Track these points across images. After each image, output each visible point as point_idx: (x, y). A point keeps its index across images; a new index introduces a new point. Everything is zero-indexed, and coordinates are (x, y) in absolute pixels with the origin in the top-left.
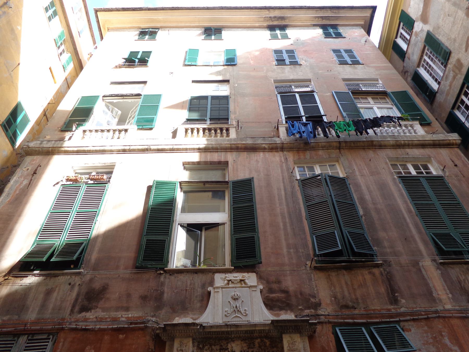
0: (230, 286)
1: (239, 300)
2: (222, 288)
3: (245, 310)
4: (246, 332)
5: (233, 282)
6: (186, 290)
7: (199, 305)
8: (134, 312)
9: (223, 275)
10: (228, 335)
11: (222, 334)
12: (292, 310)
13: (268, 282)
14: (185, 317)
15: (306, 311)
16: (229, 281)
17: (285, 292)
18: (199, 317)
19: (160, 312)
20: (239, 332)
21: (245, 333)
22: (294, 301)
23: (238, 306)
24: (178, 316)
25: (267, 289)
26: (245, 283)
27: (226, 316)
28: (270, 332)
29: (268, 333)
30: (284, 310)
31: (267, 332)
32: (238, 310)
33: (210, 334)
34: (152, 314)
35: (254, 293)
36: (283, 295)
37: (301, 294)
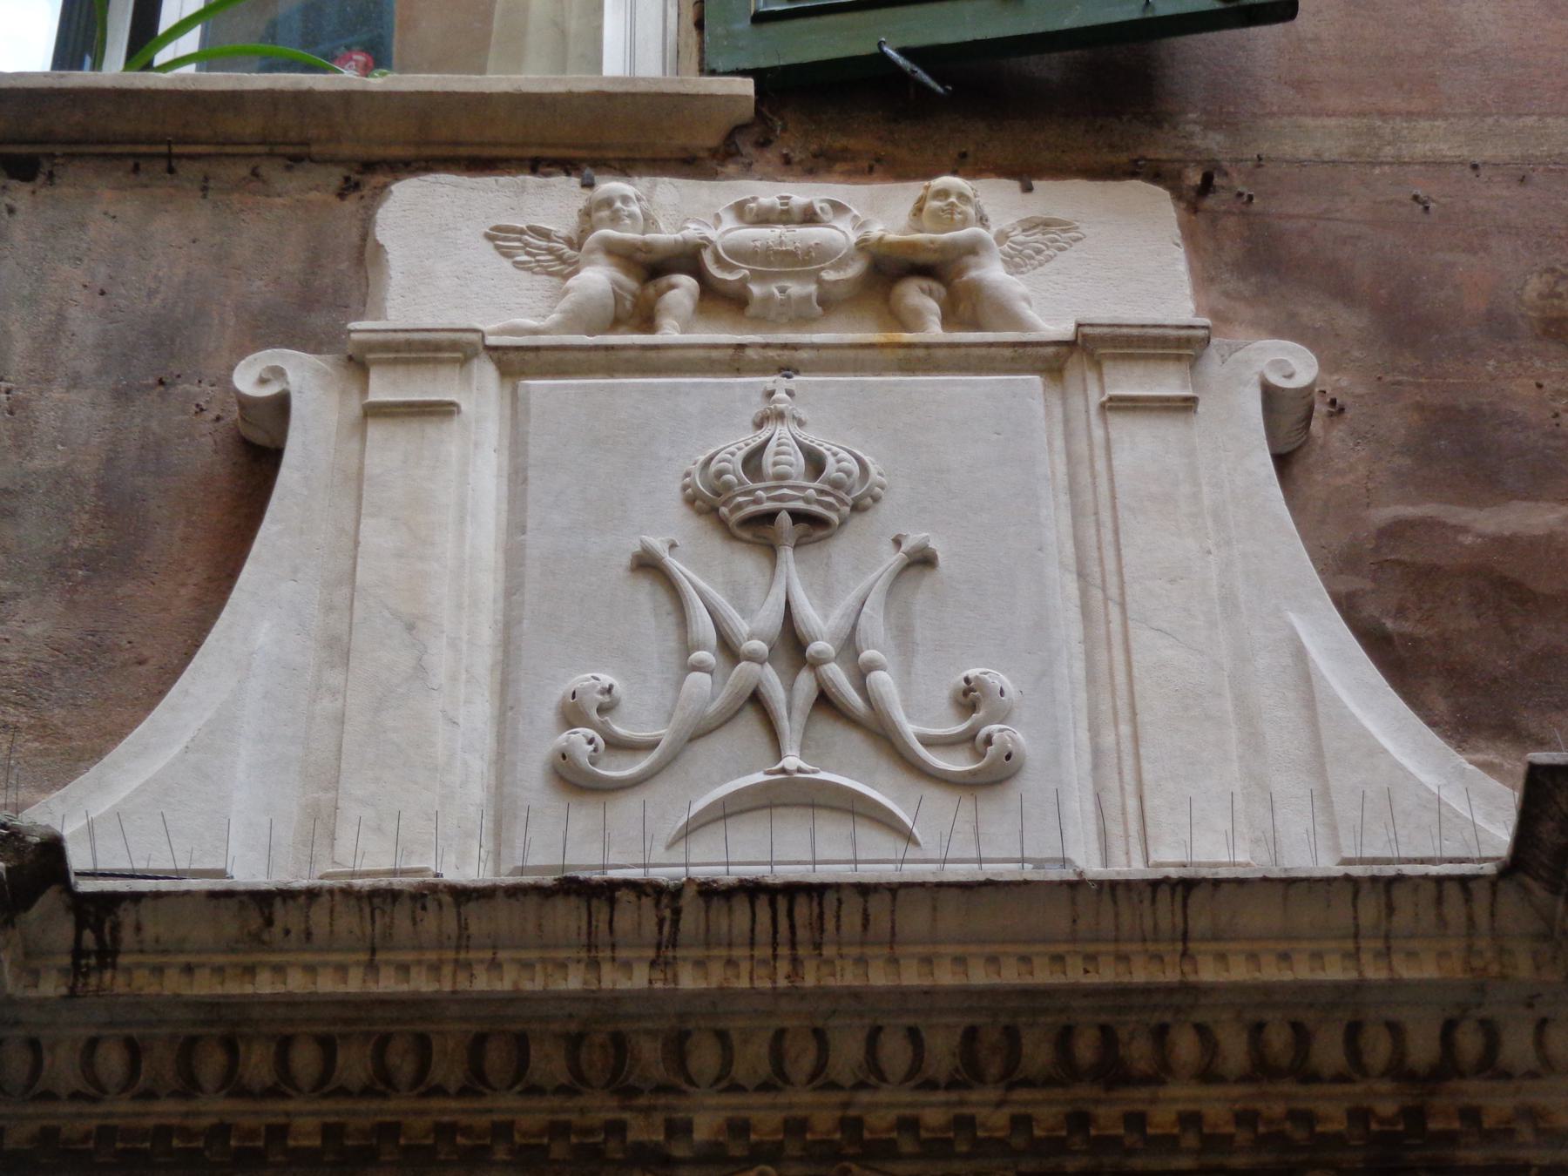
0: (670, 333)
1: (841, 549)
2: (516, 362)
3: (969, 698)
4: (991, 1038)
5: (720, 299)
10: (599, 1108)
11: (476, 1082)
13: (1405, 322)
20: (847, 1052)
21: (969, 1073)
23: (821, 625)
26: (966, 304)
27: (572, 780)
28: (1489, 1065)
29: (1447, 1067)
31: (1423, 1049)
32: (826, 701)
33: (232, 1084)
35: (1140, 447)
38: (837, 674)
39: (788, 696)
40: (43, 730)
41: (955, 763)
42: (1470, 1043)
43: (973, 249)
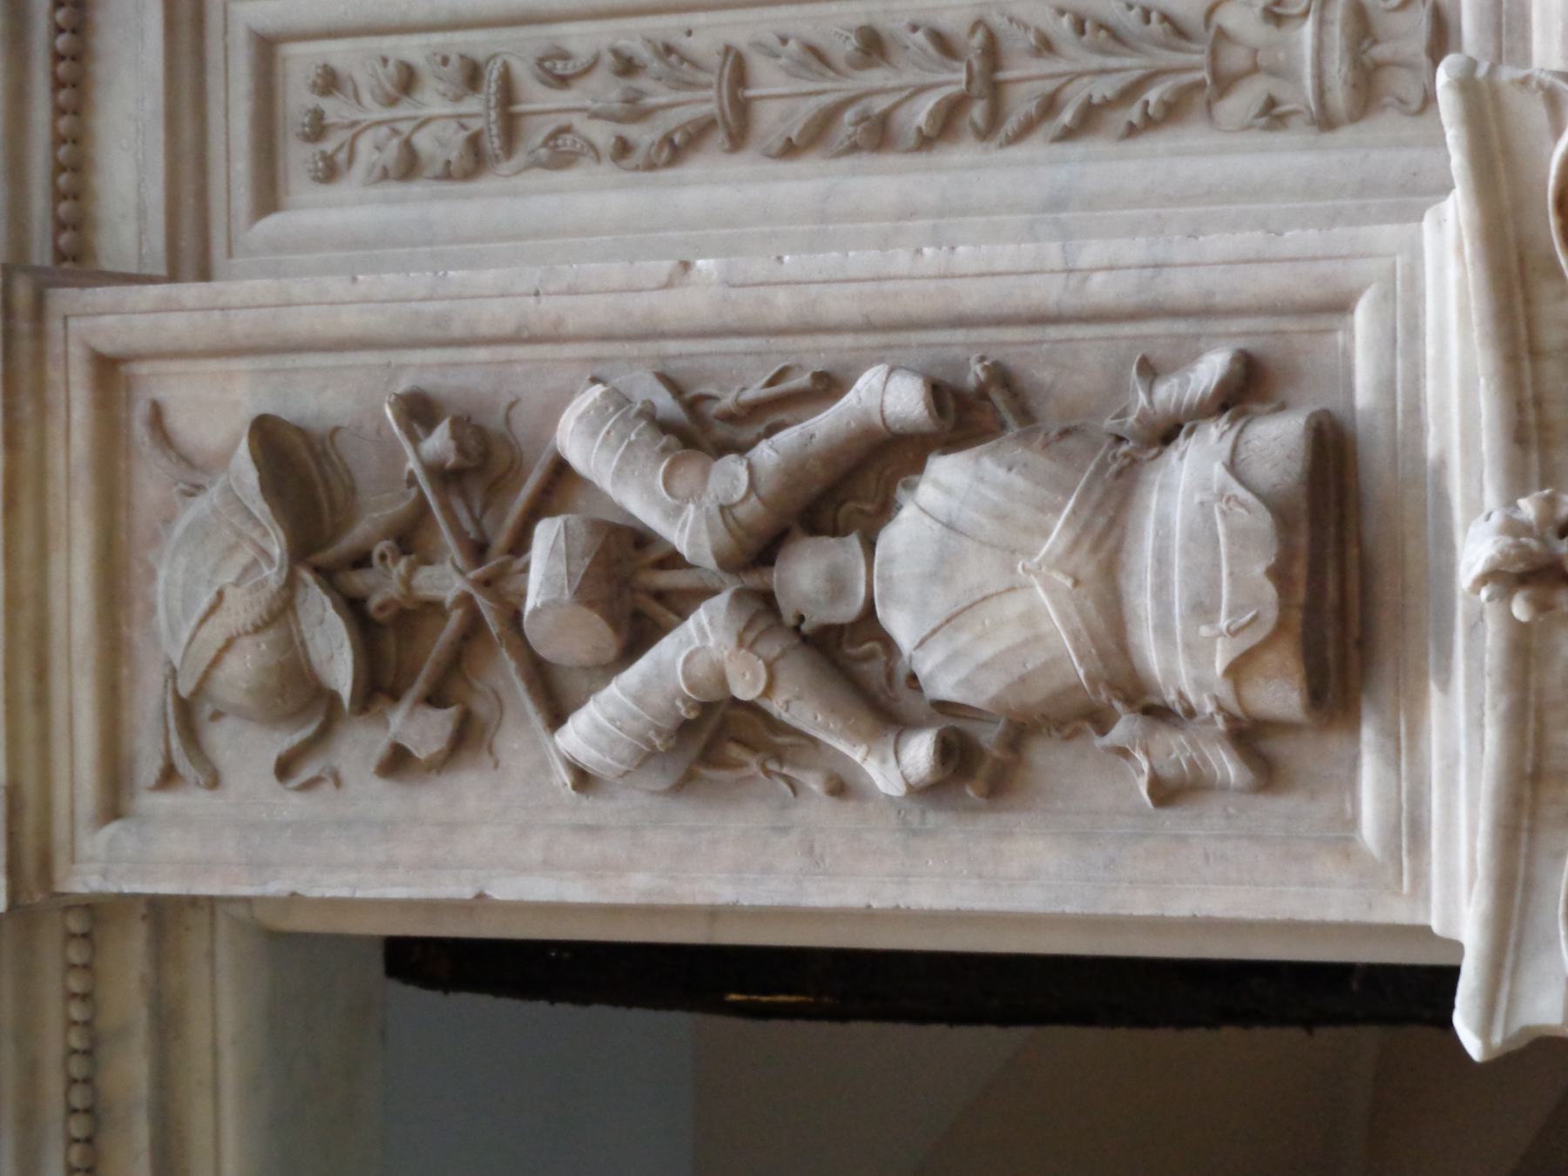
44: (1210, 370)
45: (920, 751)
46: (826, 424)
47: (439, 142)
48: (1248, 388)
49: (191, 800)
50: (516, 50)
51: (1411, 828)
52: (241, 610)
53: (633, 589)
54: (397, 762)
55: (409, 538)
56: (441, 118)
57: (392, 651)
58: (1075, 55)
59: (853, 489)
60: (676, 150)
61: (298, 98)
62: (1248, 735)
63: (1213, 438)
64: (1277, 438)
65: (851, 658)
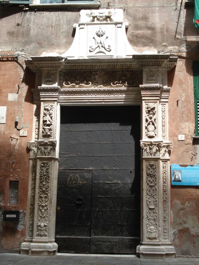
2: (87, 24)
5: (98, 19)
6: (52, 26)
7: (64, 40)
8: (4, 47)
9: (88, 11)
12: (155, 47)
13: (135, 19)
14: (51, 51)
15: (169, 48)
16: (94, 17)
17: (152, 29)
18: (64, 52)
19: (28, 47)
22: (158, 38)
24: (44, 51)
25: (133, 26)
26: (111, 20)
27: (90, 51)
29: (130, 66)
30: (148, 46)
31: (128, 66)
32: (102, 46)
34: (21, 49)
36: (149, 32)
37: (167, 31)
38: (103, 45)
39: (100, 46)
40: (65, 47)
41: (108, 50)
42: (131, 65)
43: (111, 16)
44: (156, 134)
45: (147, 126)
46: (155, 123)
47: (163, 110)
48: (156, 135)
49: (145, 104)
50: (165, 112)
51: (145, 139)
52: (150, 107)
53: (151, 118)
54: (146, 111)
55: (152, 112)
56: (163, 110)
57: (149, 111)
58: (164, 128)
59: (153, 124)
60: (162, 117)
61: (164, 105)
62: (147, 135)
63: (154, 134)
64: (154, 136)
65: (149, 124)
